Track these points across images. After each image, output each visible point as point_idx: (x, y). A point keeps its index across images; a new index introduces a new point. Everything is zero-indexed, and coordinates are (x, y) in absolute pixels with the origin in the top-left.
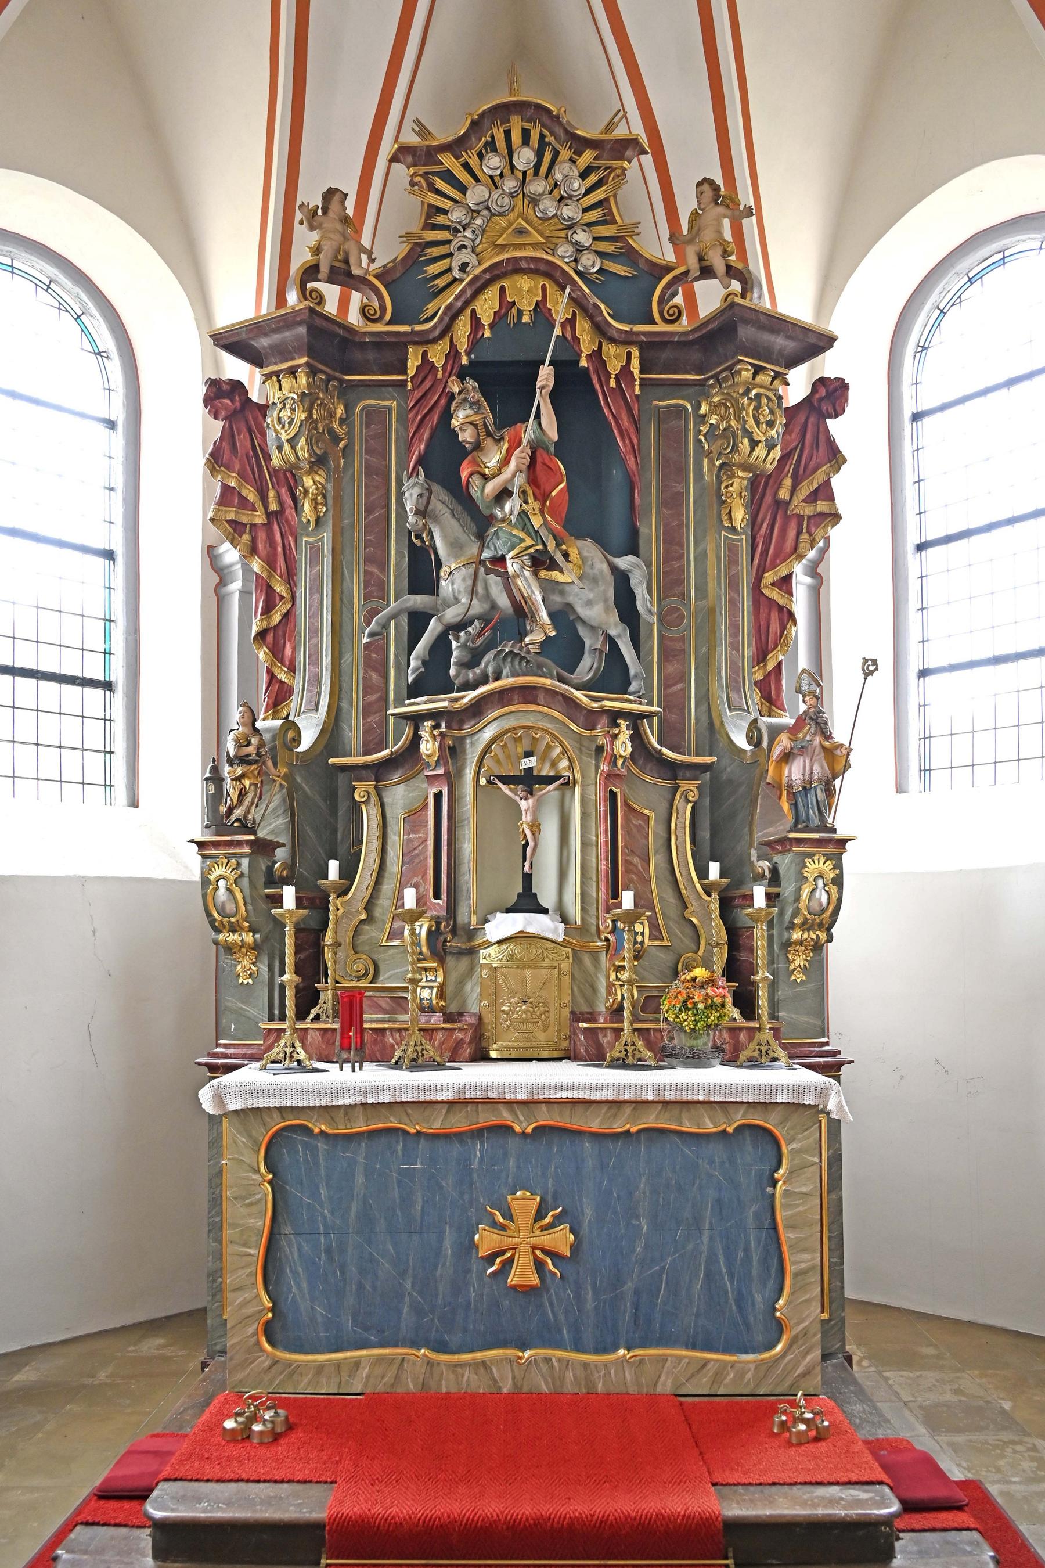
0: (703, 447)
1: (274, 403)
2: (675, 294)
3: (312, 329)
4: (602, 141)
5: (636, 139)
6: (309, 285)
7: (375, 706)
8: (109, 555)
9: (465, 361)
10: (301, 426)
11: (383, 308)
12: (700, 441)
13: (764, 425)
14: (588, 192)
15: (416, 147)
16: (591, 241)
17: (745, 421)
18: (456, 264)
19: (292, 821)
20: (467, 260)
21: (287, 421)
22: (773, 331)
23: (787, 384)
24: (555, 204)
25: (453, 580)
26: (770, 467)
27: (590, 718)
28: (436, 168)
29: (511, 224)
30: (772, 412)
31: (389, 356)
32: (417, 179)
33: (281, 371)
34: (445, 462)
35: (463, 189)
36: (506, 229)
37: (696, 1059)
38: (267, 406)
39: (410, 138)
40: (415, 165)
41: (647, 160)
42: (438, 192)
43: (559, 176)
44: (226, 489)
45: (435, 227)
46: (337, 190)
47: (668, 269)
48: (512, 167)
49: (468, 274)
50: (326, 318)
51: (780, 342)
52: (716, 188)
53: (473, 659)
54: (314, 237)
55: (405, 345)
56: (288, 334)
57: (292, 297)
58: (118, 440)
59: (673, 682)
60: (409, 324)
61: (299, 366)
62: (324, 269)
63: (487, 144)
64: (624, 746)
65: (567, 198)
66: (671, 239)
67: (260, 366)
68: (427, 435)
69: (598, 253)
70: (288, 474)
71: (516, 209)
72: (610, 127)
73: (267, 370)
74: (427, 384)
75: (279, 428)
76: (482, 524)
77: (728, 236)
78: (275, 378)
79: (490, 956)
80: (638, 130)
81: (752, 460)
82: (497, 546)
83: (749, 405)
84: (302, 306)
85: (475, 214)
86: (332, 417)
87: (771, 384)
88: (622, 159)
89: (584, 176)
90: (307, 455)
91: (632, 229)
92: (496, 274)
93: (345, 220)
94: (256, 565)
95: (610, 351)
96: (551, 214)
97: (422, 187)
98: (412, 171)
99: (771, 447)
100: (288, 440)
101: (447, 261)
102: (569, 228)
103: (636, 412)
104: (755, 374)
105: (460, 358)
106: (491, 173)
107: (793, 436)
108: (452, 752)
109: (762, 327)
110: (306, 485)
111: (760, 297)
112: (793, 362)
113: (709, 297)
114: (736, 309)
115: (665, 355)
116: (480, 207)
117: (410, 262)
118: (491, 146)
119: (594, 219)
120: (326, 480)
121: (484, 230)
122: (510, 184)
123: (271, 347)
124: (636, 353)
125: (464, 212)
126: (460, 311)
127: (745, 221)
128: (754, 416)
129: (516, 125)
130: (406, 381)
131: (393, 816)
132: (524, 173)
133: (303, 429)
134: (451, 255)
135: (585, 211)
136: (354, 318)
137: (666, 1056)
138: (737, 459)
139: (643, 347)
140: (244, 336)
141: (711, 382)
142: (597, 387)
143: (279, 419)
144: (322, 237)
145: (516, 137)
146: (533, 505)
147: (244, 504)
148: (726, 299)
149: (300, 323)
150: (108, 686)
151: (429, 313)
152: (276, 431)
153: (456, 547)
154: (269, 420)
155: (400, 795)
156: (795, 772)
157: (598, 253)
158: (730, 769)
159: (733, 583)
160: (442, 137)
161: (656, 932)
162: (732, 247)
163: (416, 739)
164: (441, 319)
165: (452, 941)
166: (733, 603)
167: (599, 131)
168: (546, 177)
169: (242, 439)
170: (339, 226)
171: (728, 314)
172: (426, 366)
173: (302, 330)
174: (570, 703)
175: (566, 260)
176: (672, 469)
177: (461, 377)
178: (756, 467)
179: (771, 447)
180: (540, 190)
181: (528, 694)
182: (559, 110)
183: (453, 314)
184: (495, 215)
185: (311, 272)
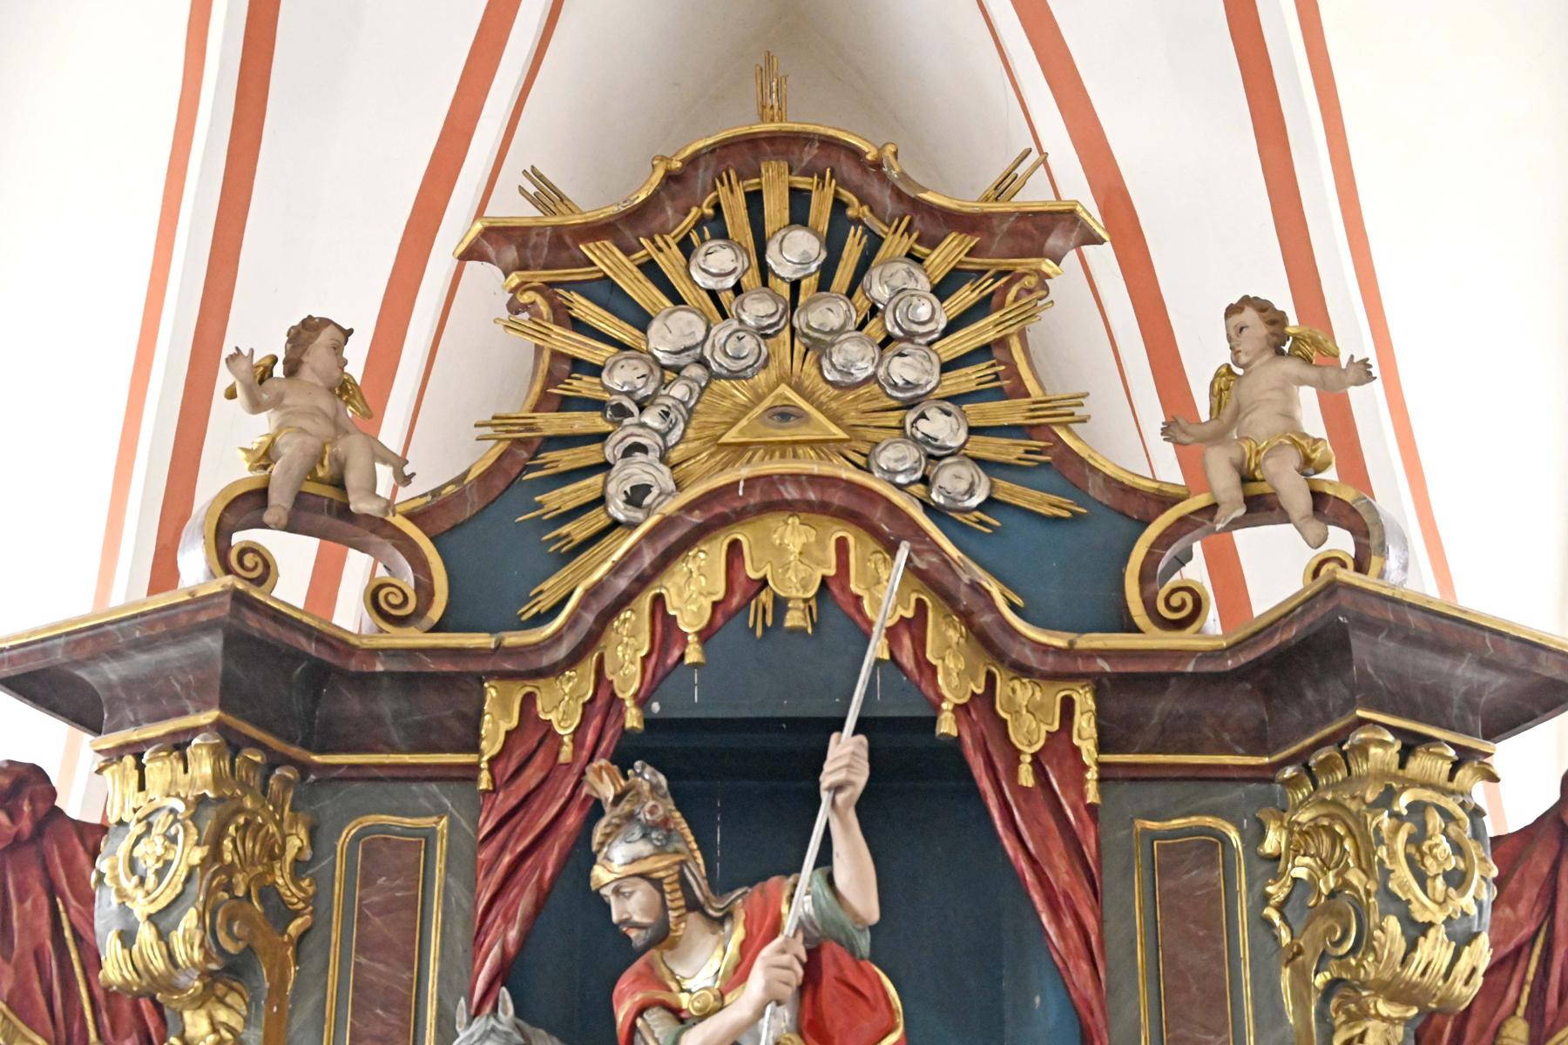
0: (1277, 938)
1: (121, 823)
2: (1184, 558)
3: (236, 641)
4: (988, 216)
5: (1072, 212)
6: (238, 538)
9: (633, 719)
10: (188, 879)
11: (425, 590)
12: (1268, 923)
13: (1440, 882)
14: (952, 327)
15: (528, 229)
16: (962, 435)
17: (1387, 873)
18: (617, 488)
20: (647, 479)
21: (150, 866)
22: (1443, 649)
23: (1494, 778)
24: (872, 352)
26: (1465, 992)
28: (578, 274)
29: (760, 398)
30: (1458, 849)
31: (435, 706)
32: (526, 298)
33: (148, 743)
35: (642, 320)
36: (745, 409)
38: (103, 829)
39: (512, 207)
40: (523, 267)
41: (1103, 258)
42: (578, 326)
43: (880, 292)
45: (566, 404)
46: (326, 322)
47: (1165, 500)
48: (764, 271)
49: (649, 511)
50: (278, 617)
51: (1464, 673)
52: (1276, 320)
54: (260, 427)
55: (479, 679)
56: (172, 652)
57: (195, 568)
60: (492, 631)
61: (195, 731)
62: (280, 500)
63: (701, 222)
65: (900, 340)
66: (1167, 432)
67: (96, 729)
68: (525, 904)
69: (980, 462)
70: (145, 1004)
71: (773, 364)
72: (1002, 189)
73: (111, 740)
74: (531, 777)
75: (129, 884)
77: (1312, 423)
78: (129, 760)
80: (1075, 188)
81: (1413, 973)
83: (1395, 831)
84: (215, 587)
85: (669, 375)
86: (273, 857)
87: (1451, 778)
88: (1040, 254)
89: (942, 290)
90: (197, 955)
91: (1070, 410)
92: (717, 515)
93: (343, 388)
96: (861, 376)
97: (540, 316)
98: (515, 279)
99: (1463, 939)
100: (150, 917)
101: (597, 479)
102: (909, 405)
103: (1090, 851)
104: (1406, 753)
105: (621, 714)
106: (711, 283)
107: (1523, 908)
109: (1415, 640)
110: (190, 1032)
111: (1405, 568)
112: (1505, 723)
113: (1276, 566)
114: (1344, 598)
115: (1163, 706)
116: (683, 359)
117: (500, 483)
119: (972, 387)
120: (247, 1021)
121: (690, 411)
123: (128, 684)
124: (1084, 700)
125: (643, 370)
126: (625, 600)
127: (1354, 393)
128: (1410, 859)
130: (476, 767)
132: (795, 286)
133: (194, 887)
134: (606, 466)
135: (946, 367)
136: (350, 614)
138: (1370, 968)
139: (1102, 687)
140: (59, 657)
141: (1289, 772)
142: (986, 785)
143: (132, 864)
144: (280, 428)
145: (776, 207)
148: (1316, 573)
149: (207, 628)
151: (545, 603)
152: (121, 893)
154: (103, 864)
157: (980, 462)
160: (592, 201)
162: (1326, 450)
164: (574, 620)
167: (980, 193)
168: (850, 294)
170: (324, 402)
171: (1320, 609)
172: (531, 725)
173: (213, 644)
175: (901, 479)
177: (622, 761)
178: (1427, 992)
179: (1463, 939)
180: (835, 321)
182: (880, 150)
184: (719, 376)
185: (249, 505)
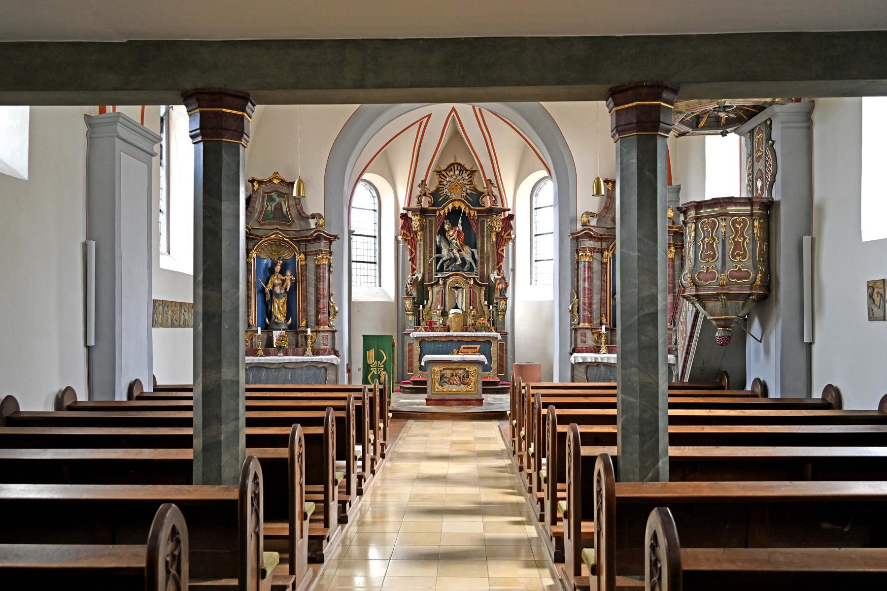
7: (430, 273)
8: (375, 237)
19: (419, 293)
25: (445, 252)
27: (467, 278)
34: (442, 232)
37: (481, 331)
53: (448, 267)
58: (377, 214)
64: (472, 282)
76: (449, 243)
79: (450, 316)
82: (452, 247)
108: (445, 283)
131: (434, 293)
137: (476, 331)
155: (436, 289)
156: (500, 286)
161: (477, 311)
165: (444, 314)
174: (464, 276)
176: (483, 231)
181: (457, 275)
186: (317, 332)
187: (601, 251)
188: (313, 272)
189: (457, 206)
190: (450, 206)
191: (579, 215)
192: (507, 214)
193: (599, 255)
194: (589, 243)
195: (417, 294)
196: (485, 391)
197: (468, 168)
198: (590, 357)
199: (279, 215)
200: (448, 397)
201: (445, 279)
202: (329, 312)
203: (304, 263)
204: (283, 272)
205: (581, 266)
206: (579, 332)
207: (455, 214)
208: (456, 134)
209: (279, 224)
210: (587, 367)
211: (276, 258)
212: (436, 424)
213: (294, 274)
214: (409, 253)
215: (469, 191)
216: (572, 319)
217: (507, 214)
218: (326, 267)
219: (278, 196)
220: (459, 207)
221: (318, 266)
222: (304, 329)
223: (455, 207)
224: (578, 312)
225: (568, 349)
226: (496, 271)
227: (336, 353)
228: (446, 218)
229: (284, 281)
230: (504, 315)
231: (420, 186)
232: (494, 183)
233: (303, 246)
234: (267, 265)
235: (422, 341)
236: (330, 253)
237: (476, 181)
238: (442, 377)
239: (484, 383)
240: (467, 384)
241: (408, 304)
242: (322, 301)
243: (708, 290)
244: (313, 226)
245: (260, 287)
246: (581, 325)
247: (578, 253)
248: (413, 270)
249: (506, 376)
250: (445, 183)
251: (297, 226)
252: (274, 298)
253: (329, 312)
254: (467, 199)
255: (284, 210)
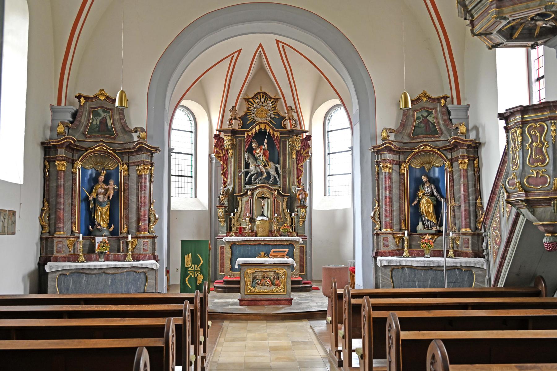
7: (240, 185)
8: (191, 155)
19: (229, 203)
25: (252, 167)
27: (272, 190)
34: (250, 150)
37: (285, 236)
44: (217, 151)
53: (255, 180)
58: (193, 135)
59: (284, 181)
64: (276, 193)
76: (256, 159)
79: (257, 223)
94: (221, 163)
95: (275, 133)
108: (252, 194)
118: (258, 98)
122: (260, 104)
129: (261, 95)
131: (243, 202)
137: (281, 236)
146: (264, 158)
147: (220, 153)
150: (191, 177)
153: (253, 163)
155: (245, 199)
156: (300, 197)
158: (292, 195)
159: (294, 167)
163: (247, 192)
165: (252, 220)
166: (293, 170)
169: (219, 144)
172: (248, 135)
174: (269, 188)
176: (285, 149)
181: (263, 187)
183: (252, 128)
186: (138, 238)
187: (399, 164)
188: (135, 182)
189: (263, 128)
190: (257, 128)
191: (379, 131)
192: (305, 135)
193: (397, 166)
194: (388, 156)
195: (229, 204)
196: (294, 290)
197: (272, 96)
198: (395, 260)
199: (104, 129)
200: (259, 298)
201: (253, 190)
202: (149, 219)
203: (126, 173)
204: (106, 182)
205: (382, 176)
206: (381, 238)
207: (261, 135)
208: (261, 68)
209: (104, 137)
210: (392, 270)
211: (100, 168)
212: (251, 325)
213: (117, 183)
214: (221, 168)
215: (273, 116)
216: (374, 225)
217: (305, 135)
218: (148, 177)
219: (104, 111)
220: (265, 129)
221: (140, 176)
222: (125, 235)
223: (260, 129)
224: (379, 218)
225: (371, 254)
226: (296, 184)
227: (155, 258)
228: (254, 138)
229: (107, 190)
230: (304, 222)
231: (231, 111)
232: (294, 109)
233: (126, 158)
234: (91, 175)
235: (233, 244)
236: (152, 164)
237: (278, 108)
238: (254, 278)
239: (293, 282)
240: (278, 285)
241: (221, 212)
242: (143, 209)
243: (539, 195)
244: (136, 139)
245: (84, 196)
246: (383, 230)
247: (378, 165)
248: (225, 183)
249: (306, 275)
250: (252, 108)
251: (120, 140)
252: (97, 206)
253: (149, 219)
254: (271, 122)
255: (109, 124)
